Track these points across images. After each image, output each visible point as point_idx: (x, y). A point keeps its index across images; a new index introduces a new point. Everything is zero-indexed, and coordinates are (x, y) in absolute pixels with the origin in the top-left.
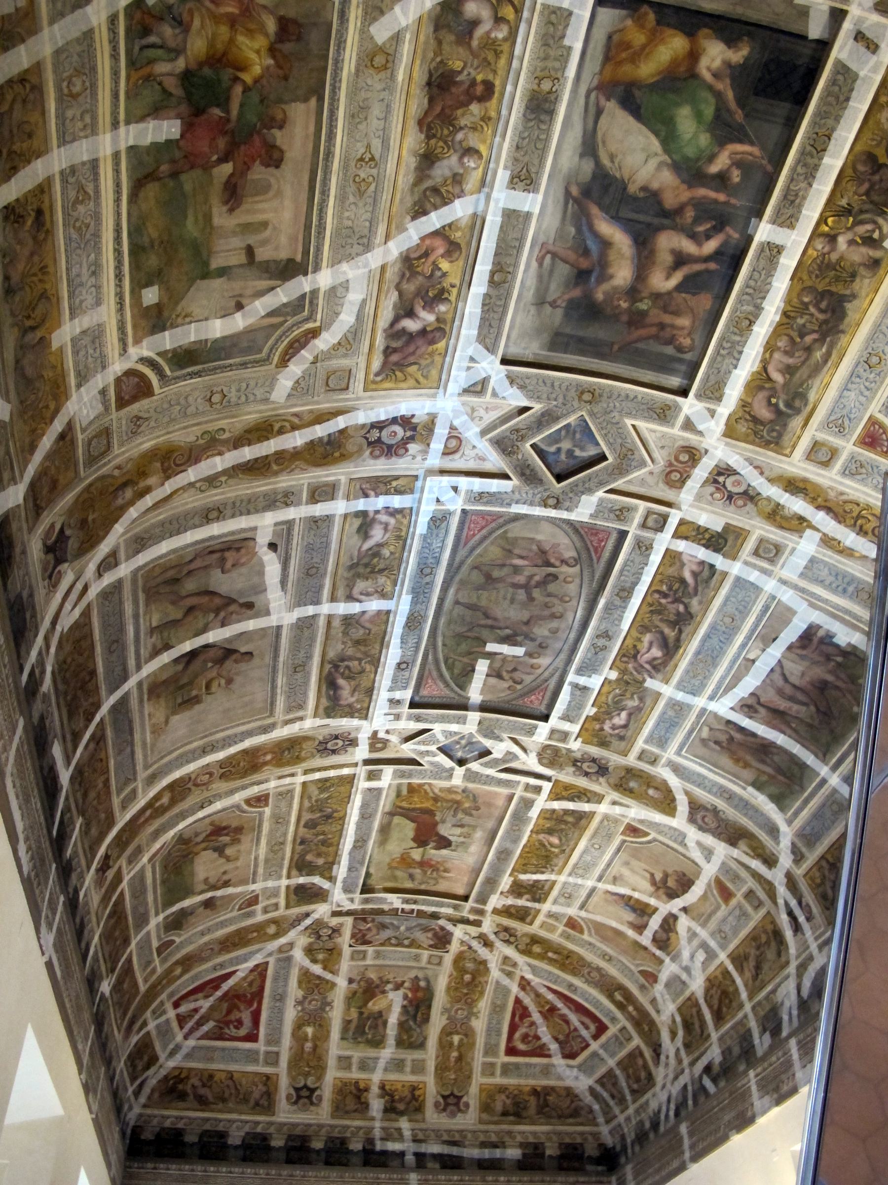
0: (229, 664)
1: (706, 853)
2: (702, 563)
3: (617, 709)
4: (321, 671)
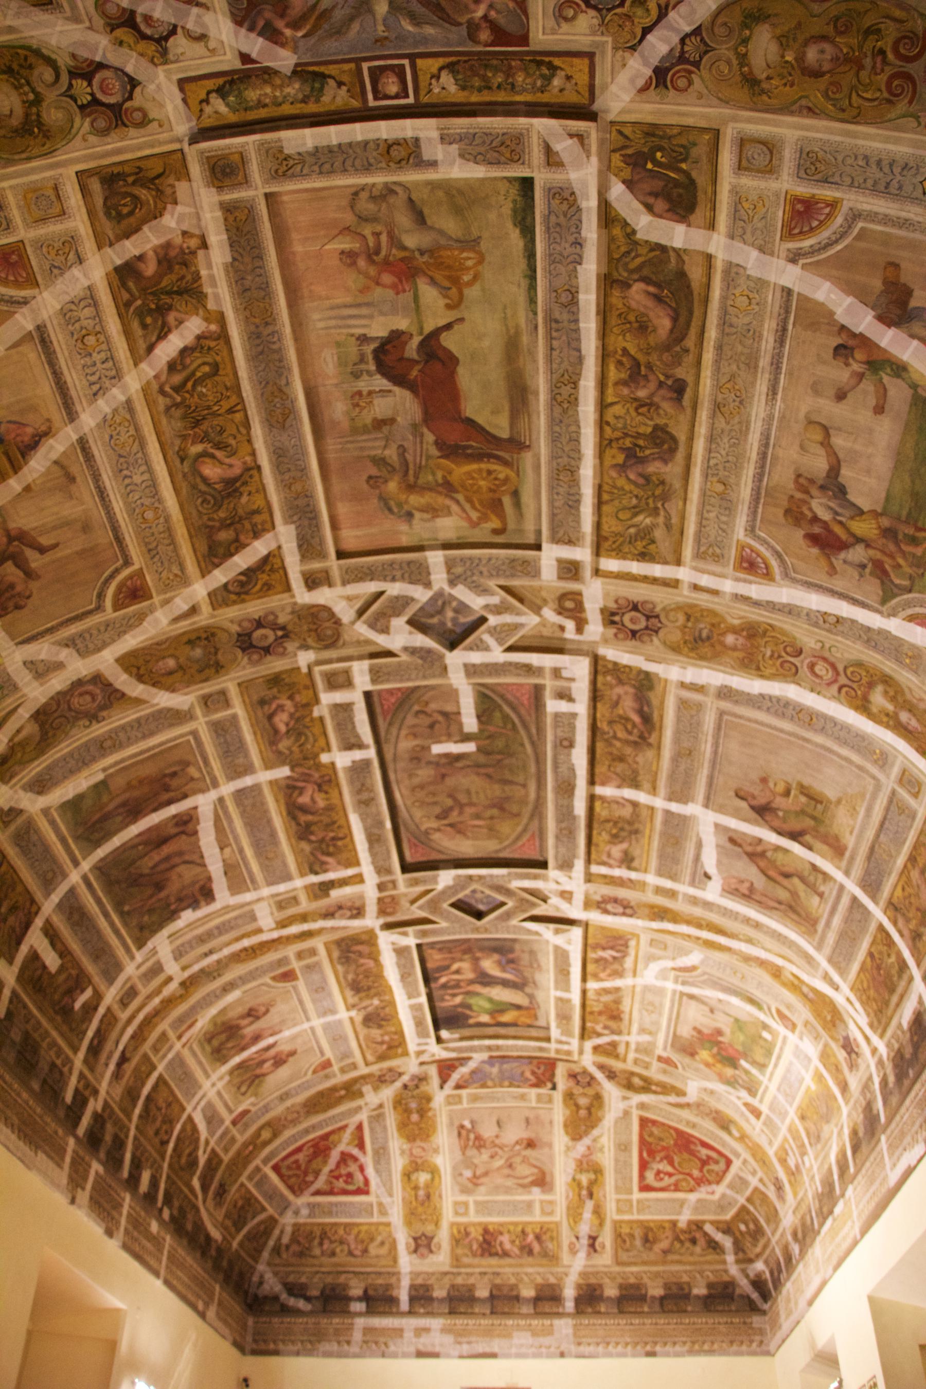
0: (761, 801)
1: (41, 668)
2: (326, 871)
3: (293, 729)
4: (660, 737)
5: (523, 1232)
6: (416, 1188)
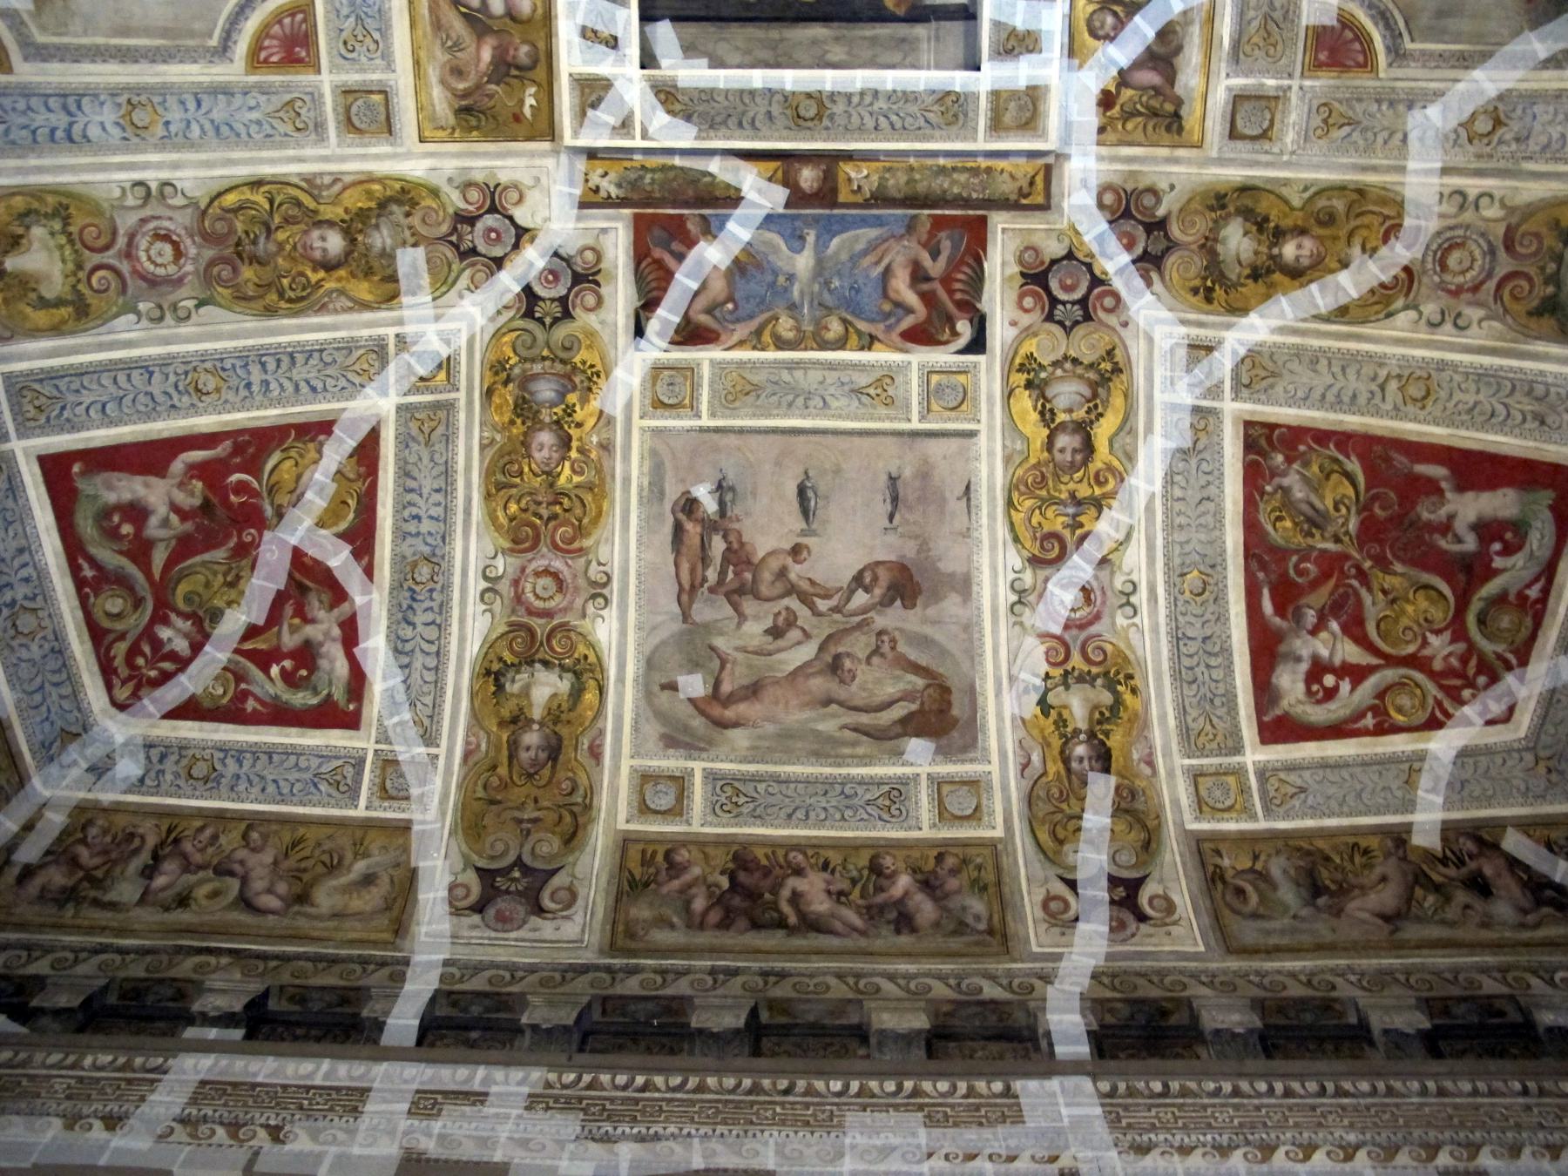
5: (875, 868)
6: (518, 721)
